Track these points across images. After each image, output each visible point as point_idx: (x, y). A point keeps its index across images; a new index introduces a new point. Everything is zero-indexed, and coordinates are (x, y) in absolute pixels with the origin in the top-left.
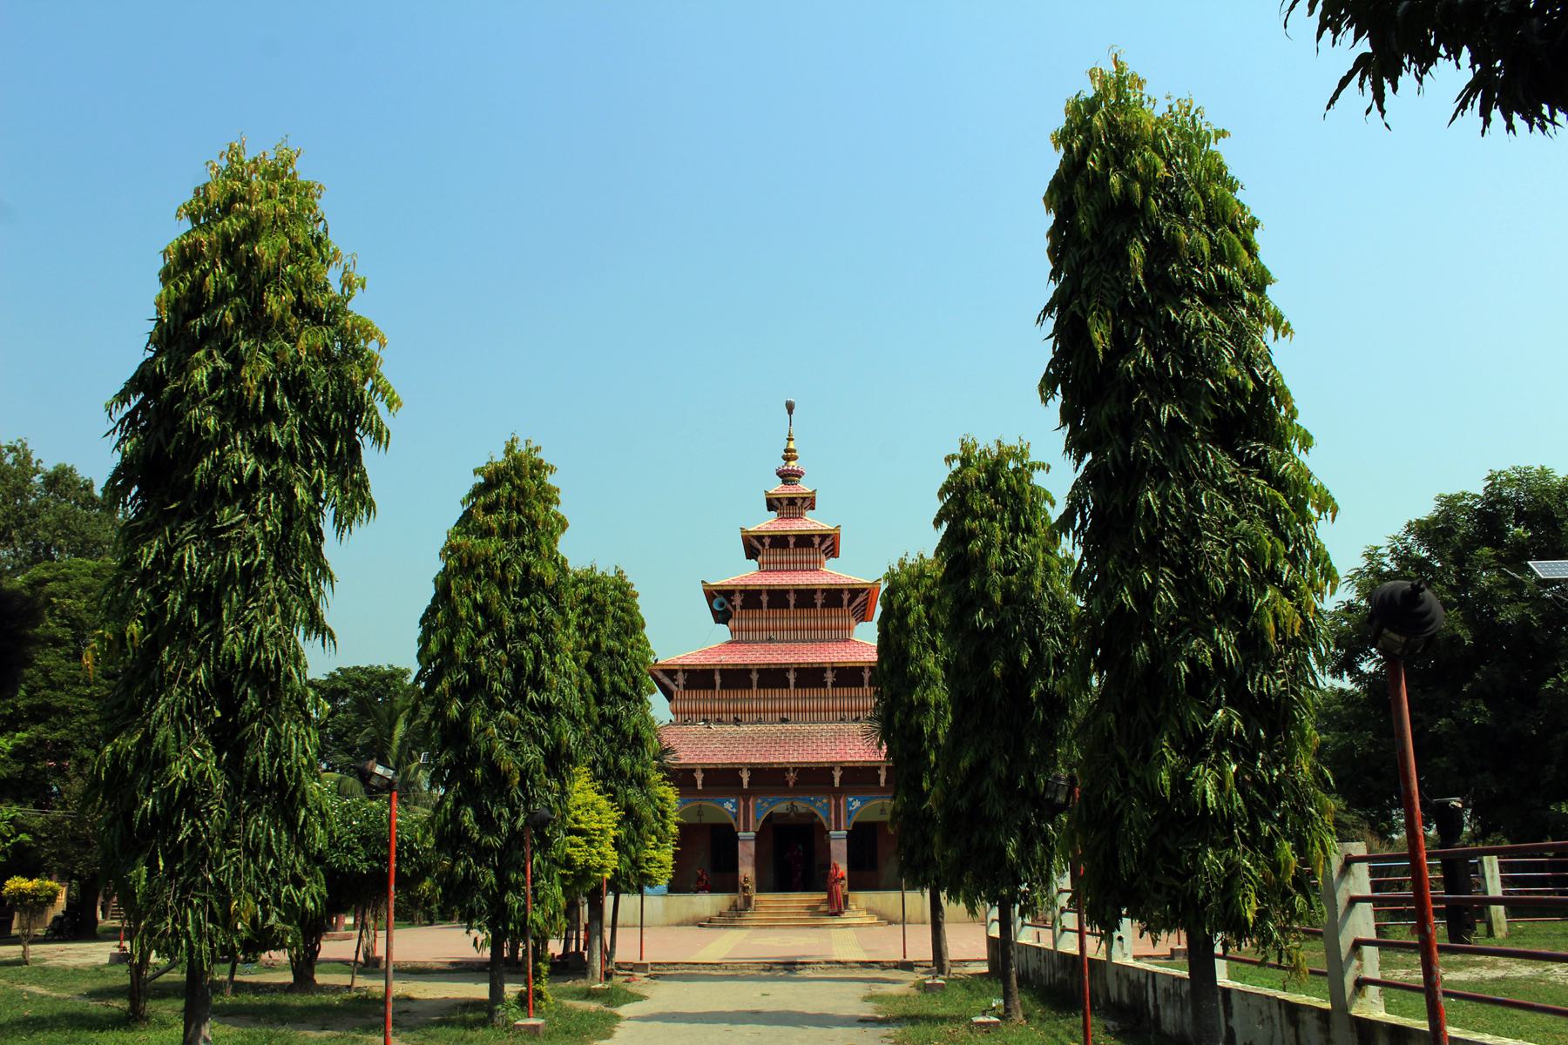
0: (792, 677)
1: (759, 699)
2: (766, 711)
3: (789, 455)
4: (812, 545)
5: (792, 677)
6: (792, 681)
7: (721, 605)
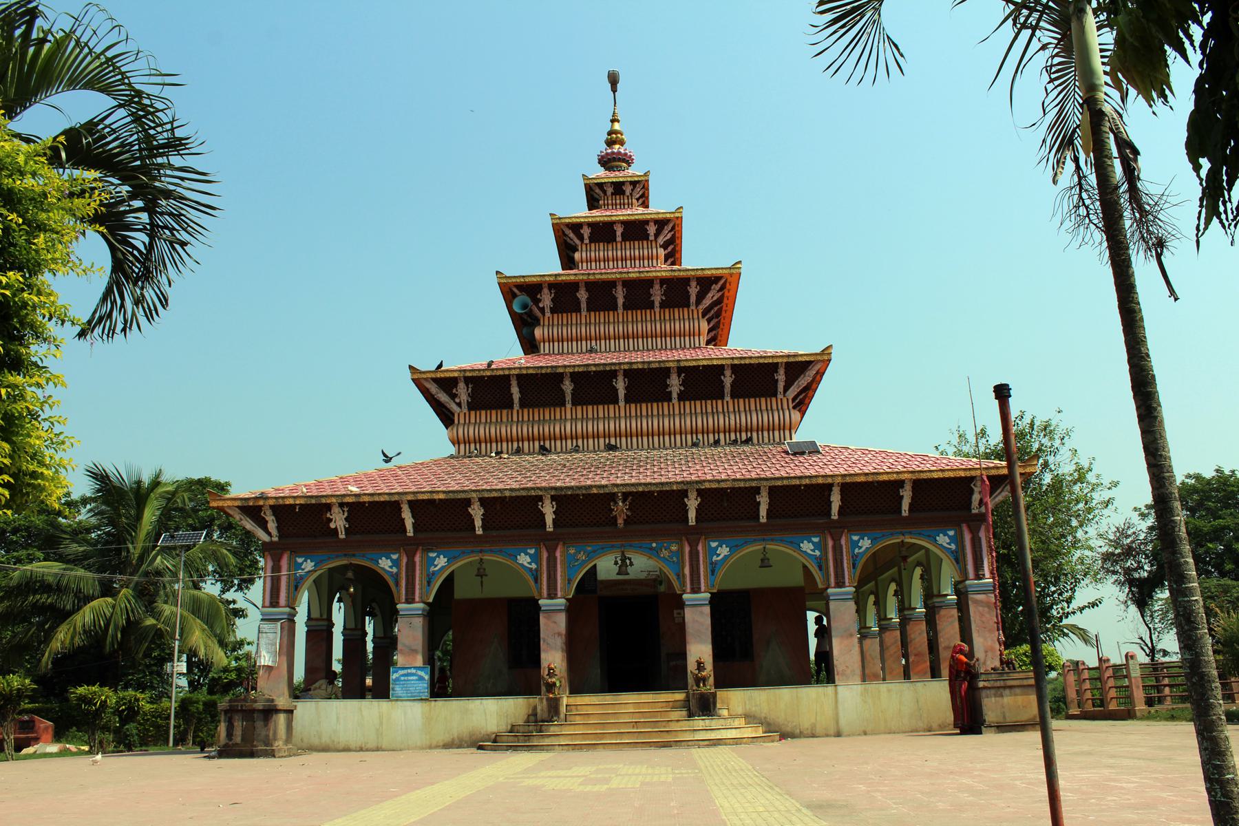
0: (620, 385)
1: (574, 420)
2: (585, 437)
4: (646, 237)
5: (620, 385)
6: (622, 393)
7: (525, 306)
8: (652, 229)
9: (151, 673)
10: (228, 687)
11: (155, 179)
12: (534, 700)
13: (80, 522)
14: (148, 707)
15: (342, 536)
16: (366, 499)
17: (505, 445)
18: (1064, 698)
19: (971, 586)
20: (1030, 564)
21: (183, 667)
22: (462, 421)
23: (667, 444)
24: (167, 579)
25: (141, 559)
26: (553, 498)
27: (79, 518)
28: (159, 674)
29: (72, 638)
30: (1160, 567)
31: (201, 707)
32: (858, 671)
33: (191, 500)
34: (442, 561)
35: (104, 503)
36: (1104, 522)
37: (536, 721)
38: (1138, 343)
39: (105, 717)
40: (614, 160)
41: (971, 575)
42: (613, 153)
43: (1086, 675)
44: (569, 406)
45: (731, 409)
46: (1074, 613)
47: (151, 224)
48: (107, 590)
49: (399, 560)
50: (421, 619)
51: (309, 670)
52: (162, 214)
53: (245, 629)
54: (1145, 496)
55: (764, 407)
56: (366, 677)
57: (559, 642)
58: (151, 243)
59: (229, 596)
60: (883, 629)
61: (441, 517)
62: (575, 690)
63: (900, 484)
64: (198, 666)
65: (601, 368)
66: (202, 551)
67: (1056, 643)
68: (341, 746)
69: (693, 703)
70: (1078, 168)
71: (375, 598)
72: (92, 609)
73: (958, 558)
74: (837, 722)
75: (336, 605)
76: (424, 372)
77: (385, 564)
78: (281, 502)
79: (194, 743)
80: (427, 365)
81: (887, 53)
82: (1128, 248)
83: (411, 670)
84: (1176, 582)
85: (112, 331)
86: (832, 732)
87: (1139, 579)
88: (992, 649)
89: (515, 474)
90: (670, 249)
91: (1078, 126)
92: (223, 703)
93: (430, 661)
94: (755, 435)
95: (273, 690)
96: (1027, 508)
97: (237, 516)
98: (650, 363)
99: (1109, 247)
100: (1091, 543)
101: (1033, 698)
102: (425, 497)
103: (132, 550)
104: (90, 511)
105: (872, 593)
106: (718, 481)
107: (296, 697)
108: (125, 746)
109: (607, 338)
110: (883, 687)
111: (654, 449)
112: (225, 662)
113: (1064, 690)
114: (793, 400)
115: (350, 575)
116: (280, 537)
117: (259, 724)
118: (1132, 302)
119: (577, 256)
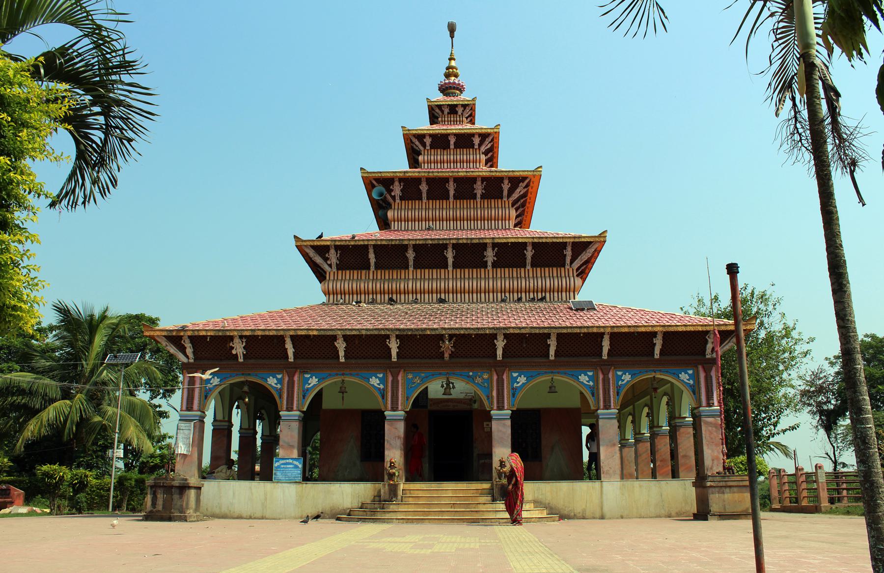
0: (450, 255)
2: (422, 292)
3: (450, 72)
4: (472, 146)
5: (450, 255)
6: (450, 261)
7: (381, 194)
8: (477, 140)
9: (97, 457)
10: (155, 468)
11: (110, 91)
12: (379, 485)
13: (47, 344)
14: (94, 482)
15: (241, 360)
16: (260, 333)
17: (363, 296)
18: (769, 496)
19: (703, 411)
20: (748, 397)
21: (121, 453)
22: (332, 278)
23: (483, 300)
24: (110, 388)
25: (92, 372)
26: (397, 337)
27: (47, 341)
28: (103, 458)
29: (40, 430)
30: (844, 402)
31: (133, 483)
32: (618, 472)
33: (130, 330)
34: (314, 381)
35: (66, 330)
36: (803, 367)
37: (380, 501)
38: (834, 236)
39: (63, 488)
40: (450, 88)
41: (704, 403)
42: (450, 83)
43: (786, 479)
44: (411, 269)
45: (531, 275)
46: (778, 434)
47: (106, 125)
48: (66, 395)
49: (283, 378)
50: (297, 423)
51: (214, 458)
52: (114, 117)
53: (167, 426)
54: (835, 348)
55: (555, 275)
56: (255, 465)
57: (399, 443)
58: (106, 139)
59: (156, 401)
60: (637, 441)
61: (315, 348)
62: (410, 479)
63: (654, 334)
64: (131, 452)
65: (436, 242)
66: (137, 368)
67: (765, 455)
68: (236, 515)
69: (496, 490)
70: (795, 105)
71: (264, 406)
72: (55, 408)
73: (695, 390)
74: (602, 508)
75: (235, 411)
76: (305, 241)
77: (272, 381)
78: (196, 333)
79: (127, 509)
80: (309, 235)
81: (655, 14)
82: (829, 166)
83: (288, 459)
84: (856, 413)
85: (75, 204)
86: (598, 515)
87: (827, 411)
88: (718, 458)
89: (370, 318)
90: (489, 155)
91: (795, 74)
92: (150, 480)
93: (303, 454)
94: (548, 295)
95: (187, 472)
96: (747, 355)
97: (164, 343)
98: (472, 239)
99: (815, 165)
100: (793, 383)
101: (747, 496)
102: (303, 333)
103: (85, 366)
104: (55, 336)
105: (630, 414)
106: (520, 328)
107: (204, 478)
108: (77, 510)
109: (441, 220)
110: (636, 483)
111: (473, 302)
112: (152, 450)
113: (769, 490)
114: (577, 270)
115: (246, 389)
116: (195, 360)
117: (176, 497)
118: (830, 205)
119: (421, 158)
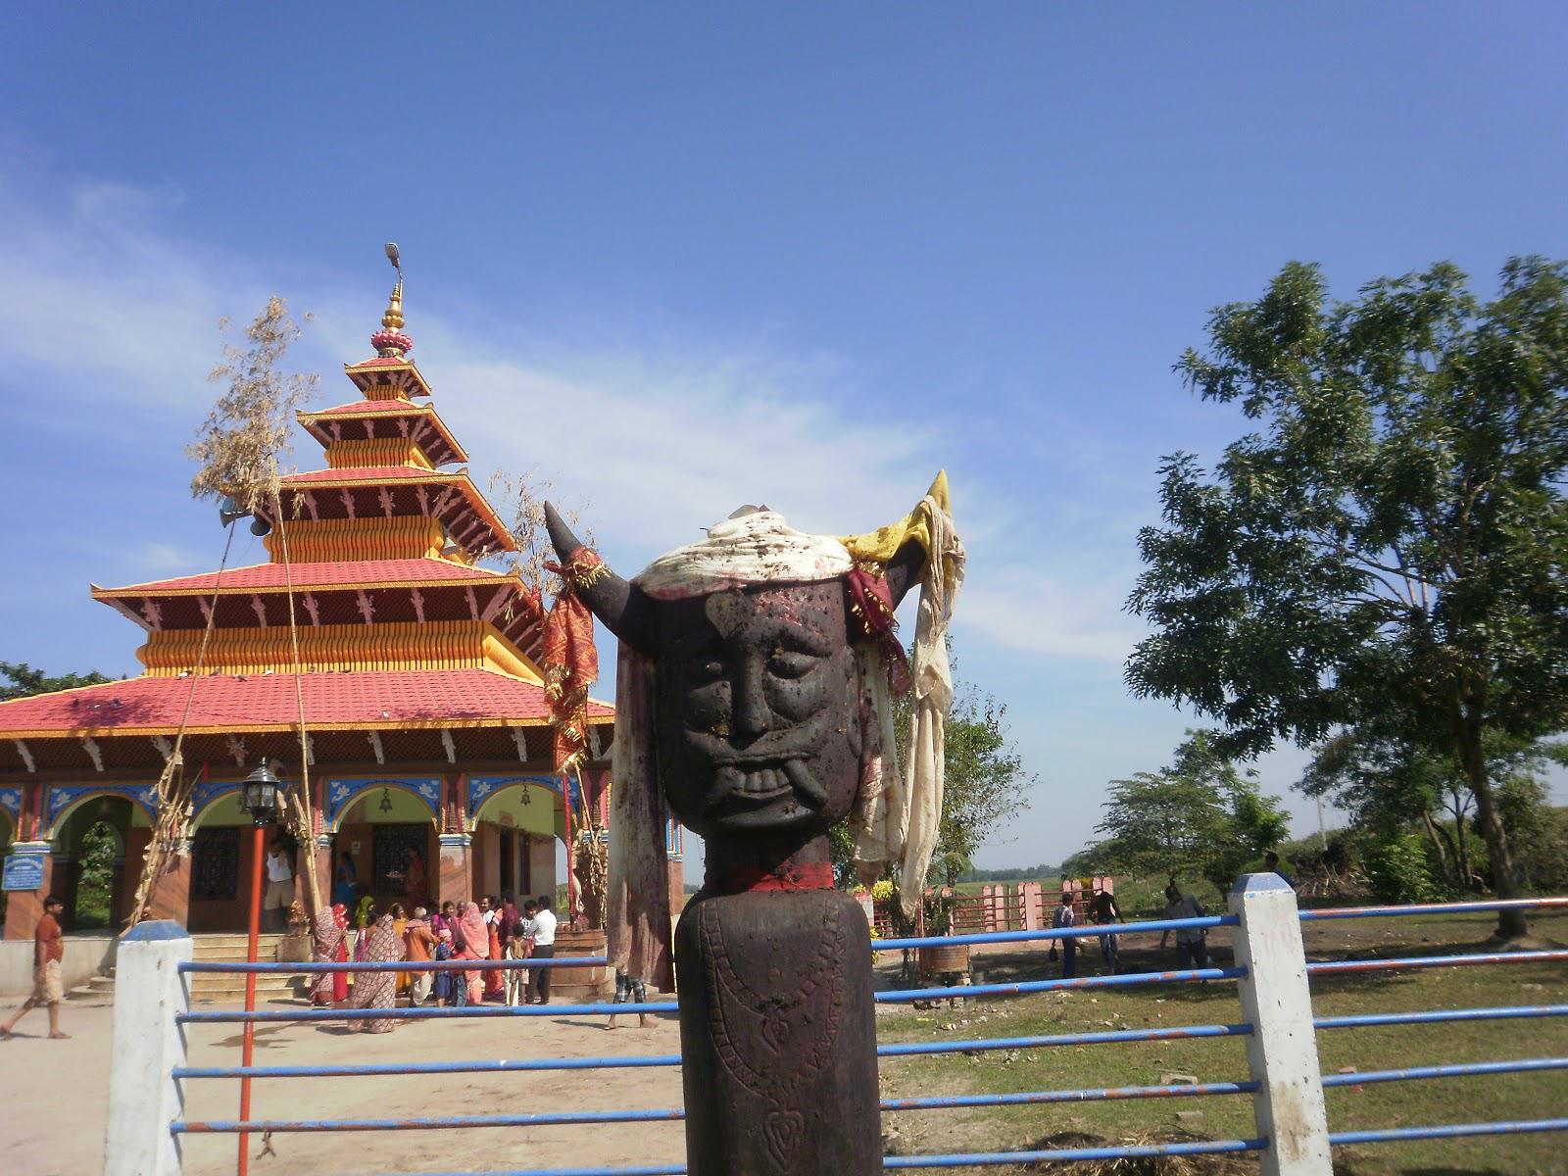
4: (398, 434)
